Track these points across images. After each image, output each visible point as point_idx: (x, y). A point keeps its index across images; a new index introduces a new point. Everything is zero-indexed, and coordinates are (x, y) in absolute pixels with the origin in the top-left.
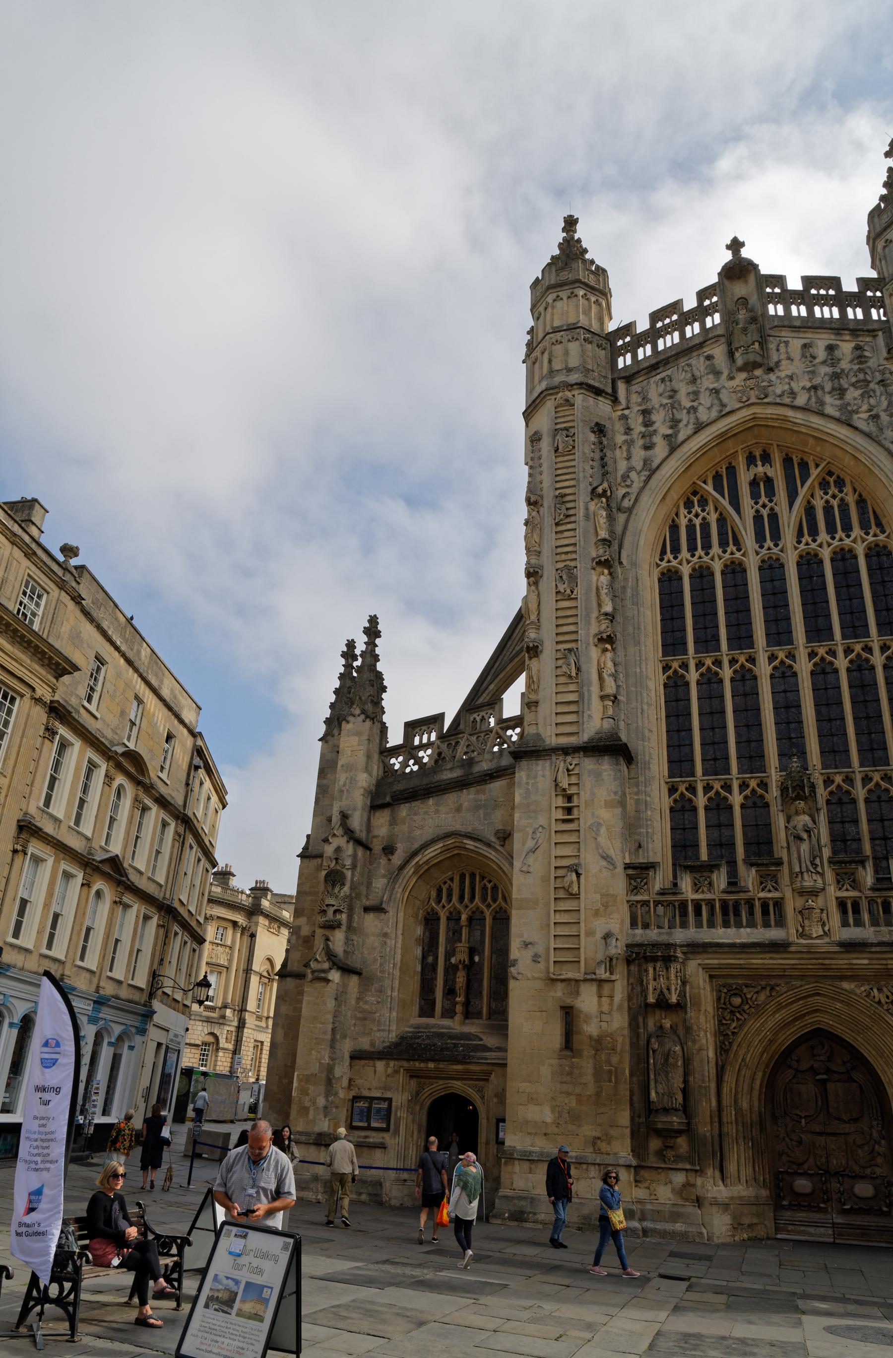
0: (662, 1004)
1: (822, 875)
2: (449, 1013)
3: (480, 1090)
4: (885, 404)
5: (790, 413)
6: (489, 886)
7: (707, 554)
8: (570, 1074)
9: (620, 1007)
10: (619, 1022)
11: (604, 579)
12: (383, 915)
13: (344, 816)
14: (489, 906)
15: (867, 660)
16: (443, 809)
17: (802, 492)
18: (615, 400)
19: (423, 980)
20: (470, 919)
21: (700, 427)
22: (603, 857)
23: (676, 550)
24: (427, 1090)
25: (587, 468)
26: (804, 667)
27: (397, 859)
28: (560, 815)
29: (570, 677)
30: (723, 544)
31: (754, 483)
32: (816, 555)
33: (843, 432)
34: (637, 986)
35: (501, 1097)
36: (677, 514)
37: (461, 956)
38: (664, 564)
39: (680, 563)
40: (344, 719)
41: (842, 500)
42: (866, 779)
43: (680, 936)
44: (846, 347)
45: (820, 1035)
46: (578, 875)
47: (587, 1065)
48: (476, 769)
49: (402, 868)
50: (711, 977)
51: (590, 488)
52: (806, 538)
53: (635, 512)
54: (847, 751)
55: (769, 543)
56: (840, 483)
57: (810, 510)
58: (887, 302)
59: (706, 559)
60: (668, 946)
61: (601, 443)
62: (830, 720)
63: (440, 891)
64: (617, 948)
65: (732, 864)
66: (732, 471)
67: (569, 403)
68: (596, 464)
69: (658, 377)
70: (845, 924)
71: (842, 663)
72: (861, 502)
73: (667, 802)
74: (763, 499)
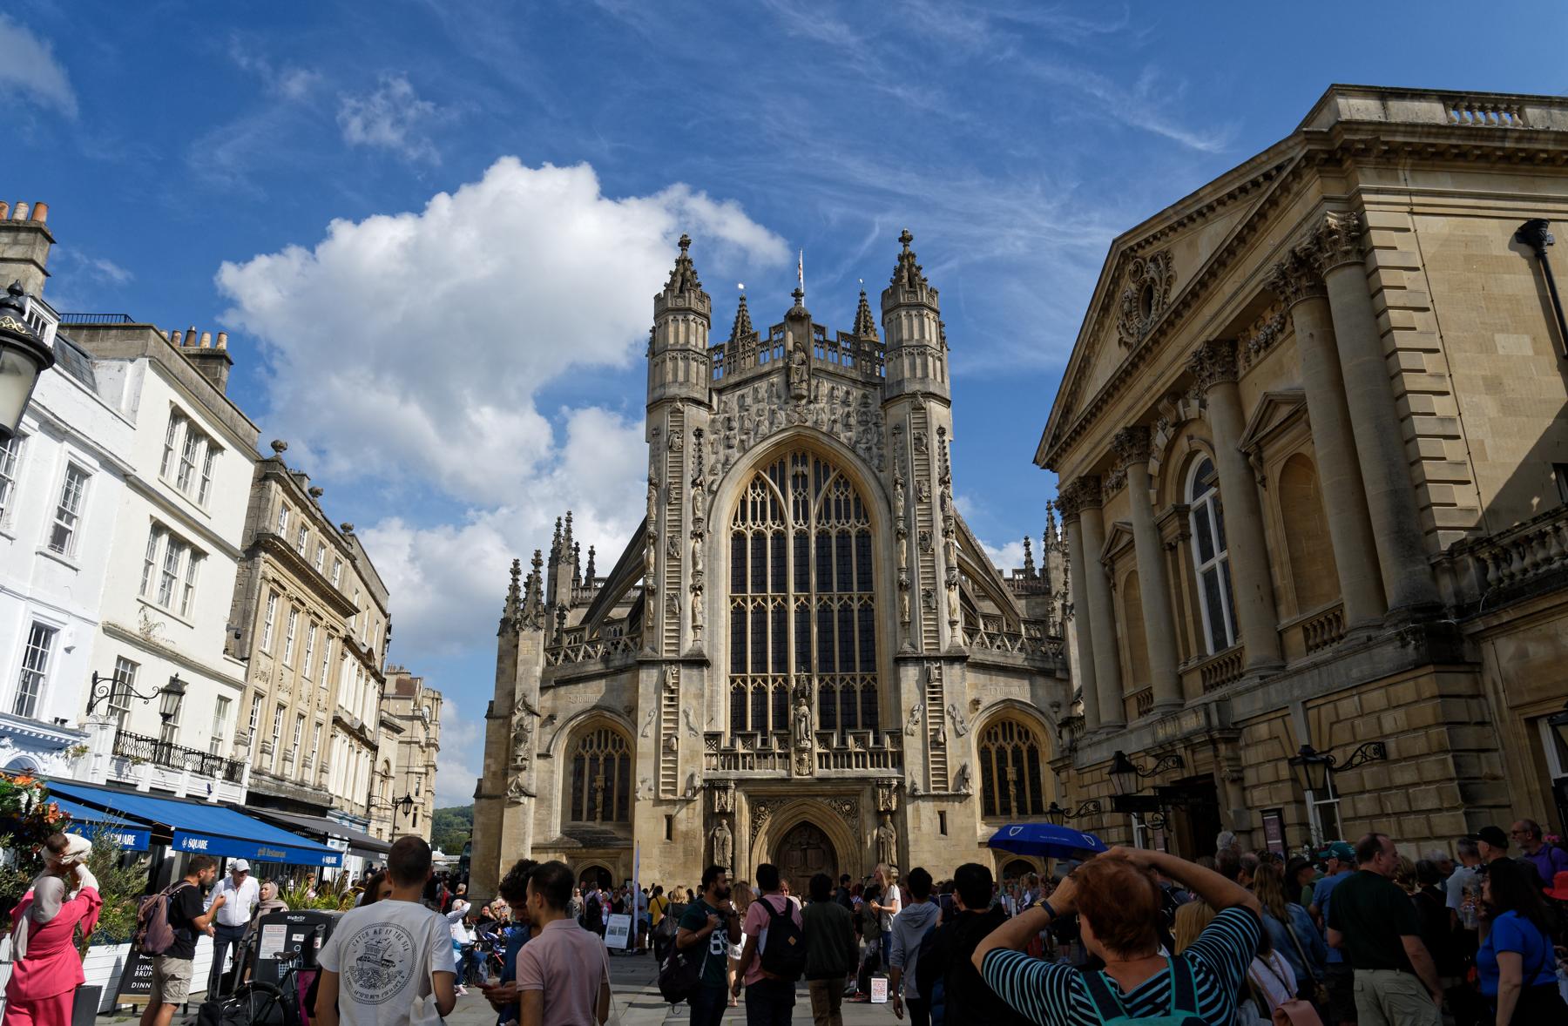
0: (723, 813)
1: (811, 741)
2: (592, 817)
3: (614, 864)
4: (876, 440)
5: (821, 436)
6: (617, 738)
7: (763, 524)
8: (670, 852)
9: (699, 815)
10: (698, 823)
11: (698, 546)
12: (549, 759)
13: (524, 696)
14: (617, 751)
15: (850, 606)
16: (589, 690)
17: (824, 488)
18: (710, 407)
19: (574, 798)
20: (605, 759)
21: (764, 439)
22: (691, 729)
23: (744, 519)
24: (581, 865)
25: (690, 463)
26: (814, 607)
27: (558, 722)
28: (667, 703)
29: (675, 613)
30: (774, 519)
31: (795, 477)
32: (828, 533)
33: (850, 455)
34: (709, 802)
35: (629, 867)
36: (746, 492)
37: (600, 782)
38: (736, 528)
39: (746, 529)
40: (521, 628)
41: (847, 496)
42: (842, 679)
43: (733, 774)
44: (856, 393)
45: (806, 825)
46: (677, 739)
47: (680, 848)
48: (612, 664)
49: (562, 728)
50: (749, 796)
51: (691, 479)
52: (824, 521)
53: (719, 494)
54: (834, 662)
55: (801, 521)
56: (846, 484)
57: (827, 500)
58: (885, 363)
59: (762, 528)
60: (728, 780)
61: (699, 444)
62: (826, 642)
63: (585, 741)
64: (698, 783)
65: (765, 733)
66: (782, 464)
67: (679, 411)
68: (696, 461)
69: (738, 393)
70: (821, 767)
71: (836, 606)
72: (857, 499)
73: (730, 688)
74: (800, 489)
